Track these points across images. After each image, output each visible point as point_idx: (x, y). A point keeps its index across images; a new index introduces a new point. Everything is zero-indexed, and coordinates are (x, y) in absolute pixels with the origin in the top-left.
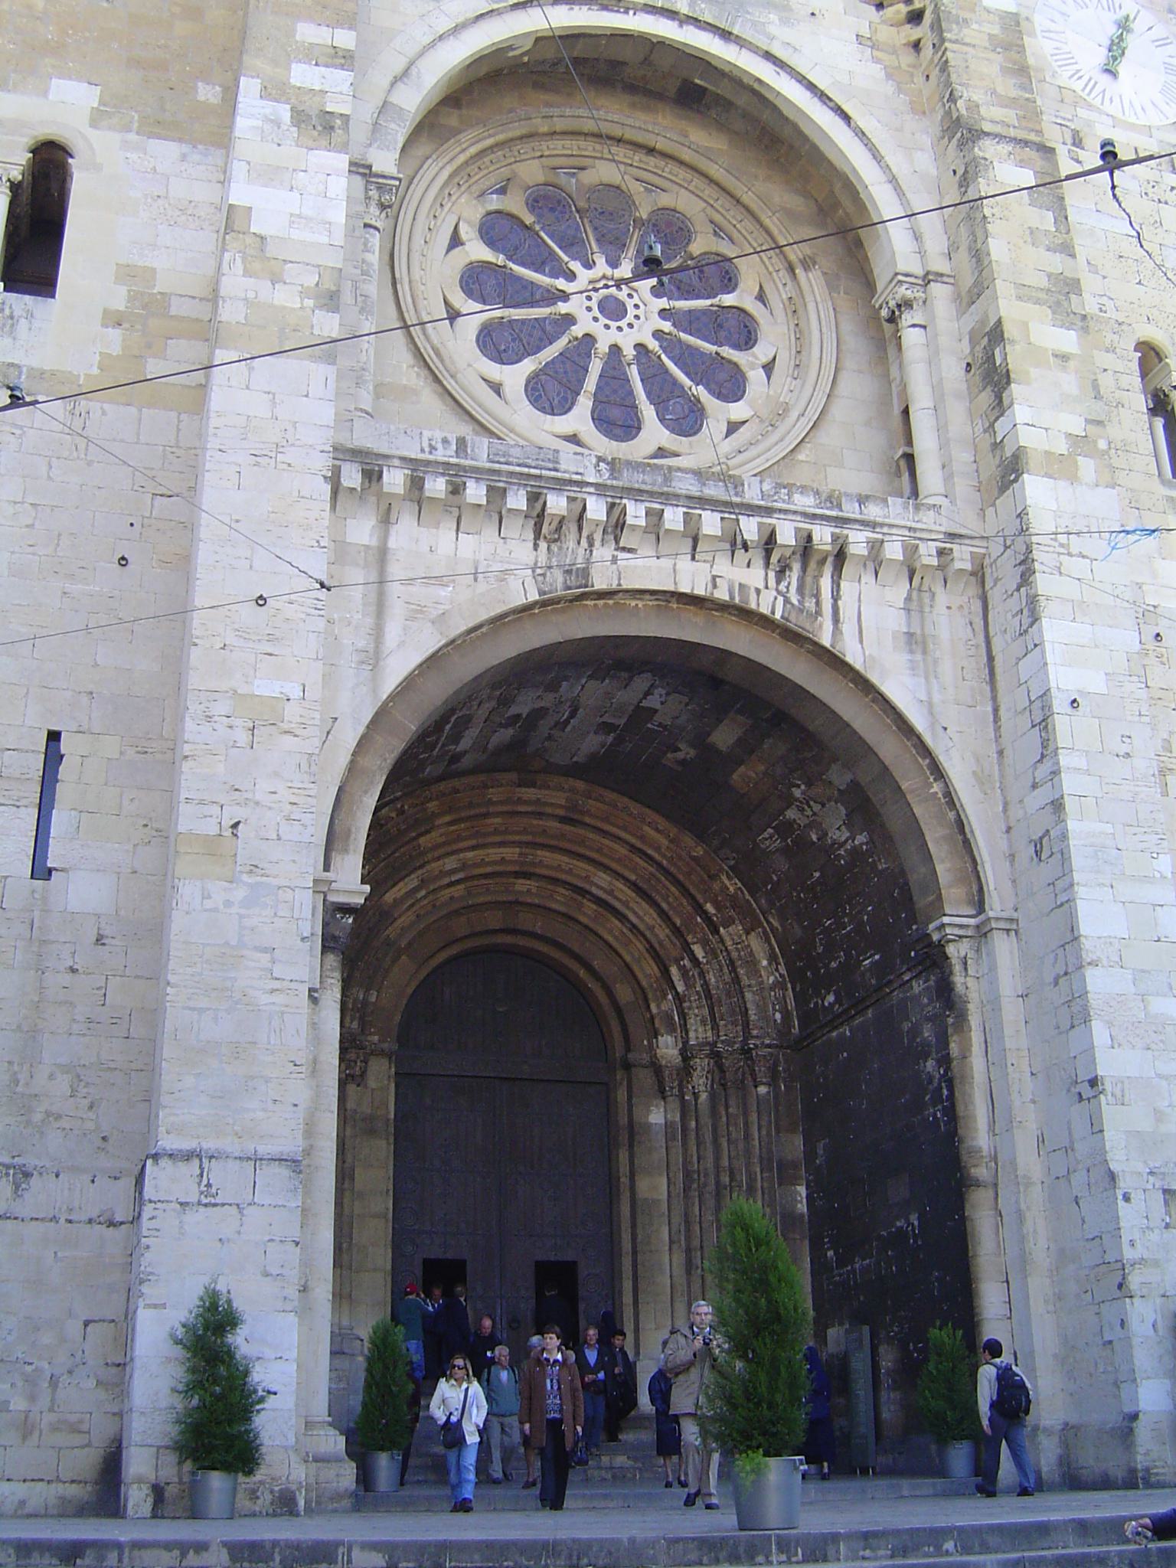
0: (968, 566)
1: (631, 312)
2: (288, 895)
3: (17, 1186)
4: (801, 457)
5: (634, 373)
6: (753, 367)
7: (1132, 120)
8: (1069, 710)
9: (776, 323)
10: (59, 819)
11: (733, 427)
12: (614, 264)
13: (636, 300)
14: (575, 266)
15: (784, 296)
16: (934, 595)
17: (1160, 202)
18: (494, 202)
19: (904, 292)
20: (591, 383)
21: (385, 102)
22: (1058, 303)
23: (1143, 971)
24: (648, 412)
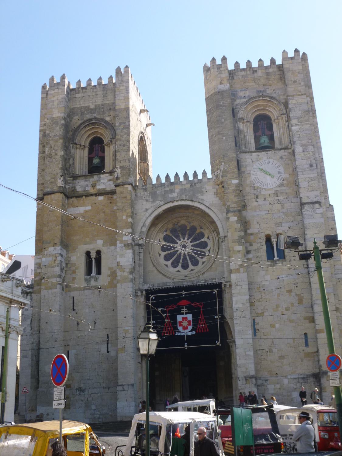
0: (229, 286)
1: (187, 246)
2: (130, 354)
3: (108, 390)
4: (212, 266)
5: (188, 257)
6: (206, 251)
7: (269, 188)
8: (236, 311)
9: (211, 242)
10: (109, 345)
11: (203, 263)
12: (184, 239)
13: (188, 244)
14: (178, 241)
15: (212, 237)
16: (225, 291)
17: (273, 204)
18: (165, 233)
19: (221, 240)
20: (181, 261)
21: (141, 231)
22: (239, 241)
23: (245, 348)
24: (190, 263)
